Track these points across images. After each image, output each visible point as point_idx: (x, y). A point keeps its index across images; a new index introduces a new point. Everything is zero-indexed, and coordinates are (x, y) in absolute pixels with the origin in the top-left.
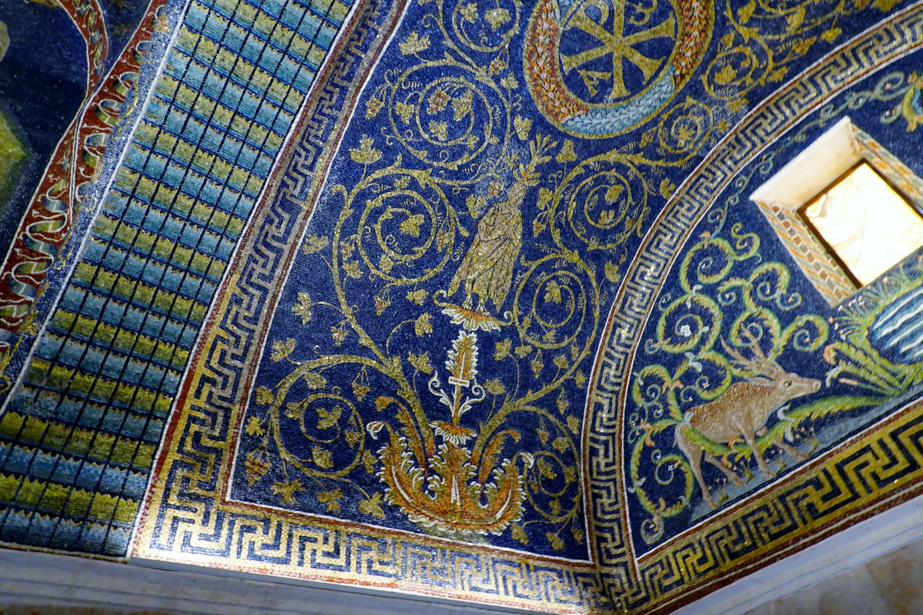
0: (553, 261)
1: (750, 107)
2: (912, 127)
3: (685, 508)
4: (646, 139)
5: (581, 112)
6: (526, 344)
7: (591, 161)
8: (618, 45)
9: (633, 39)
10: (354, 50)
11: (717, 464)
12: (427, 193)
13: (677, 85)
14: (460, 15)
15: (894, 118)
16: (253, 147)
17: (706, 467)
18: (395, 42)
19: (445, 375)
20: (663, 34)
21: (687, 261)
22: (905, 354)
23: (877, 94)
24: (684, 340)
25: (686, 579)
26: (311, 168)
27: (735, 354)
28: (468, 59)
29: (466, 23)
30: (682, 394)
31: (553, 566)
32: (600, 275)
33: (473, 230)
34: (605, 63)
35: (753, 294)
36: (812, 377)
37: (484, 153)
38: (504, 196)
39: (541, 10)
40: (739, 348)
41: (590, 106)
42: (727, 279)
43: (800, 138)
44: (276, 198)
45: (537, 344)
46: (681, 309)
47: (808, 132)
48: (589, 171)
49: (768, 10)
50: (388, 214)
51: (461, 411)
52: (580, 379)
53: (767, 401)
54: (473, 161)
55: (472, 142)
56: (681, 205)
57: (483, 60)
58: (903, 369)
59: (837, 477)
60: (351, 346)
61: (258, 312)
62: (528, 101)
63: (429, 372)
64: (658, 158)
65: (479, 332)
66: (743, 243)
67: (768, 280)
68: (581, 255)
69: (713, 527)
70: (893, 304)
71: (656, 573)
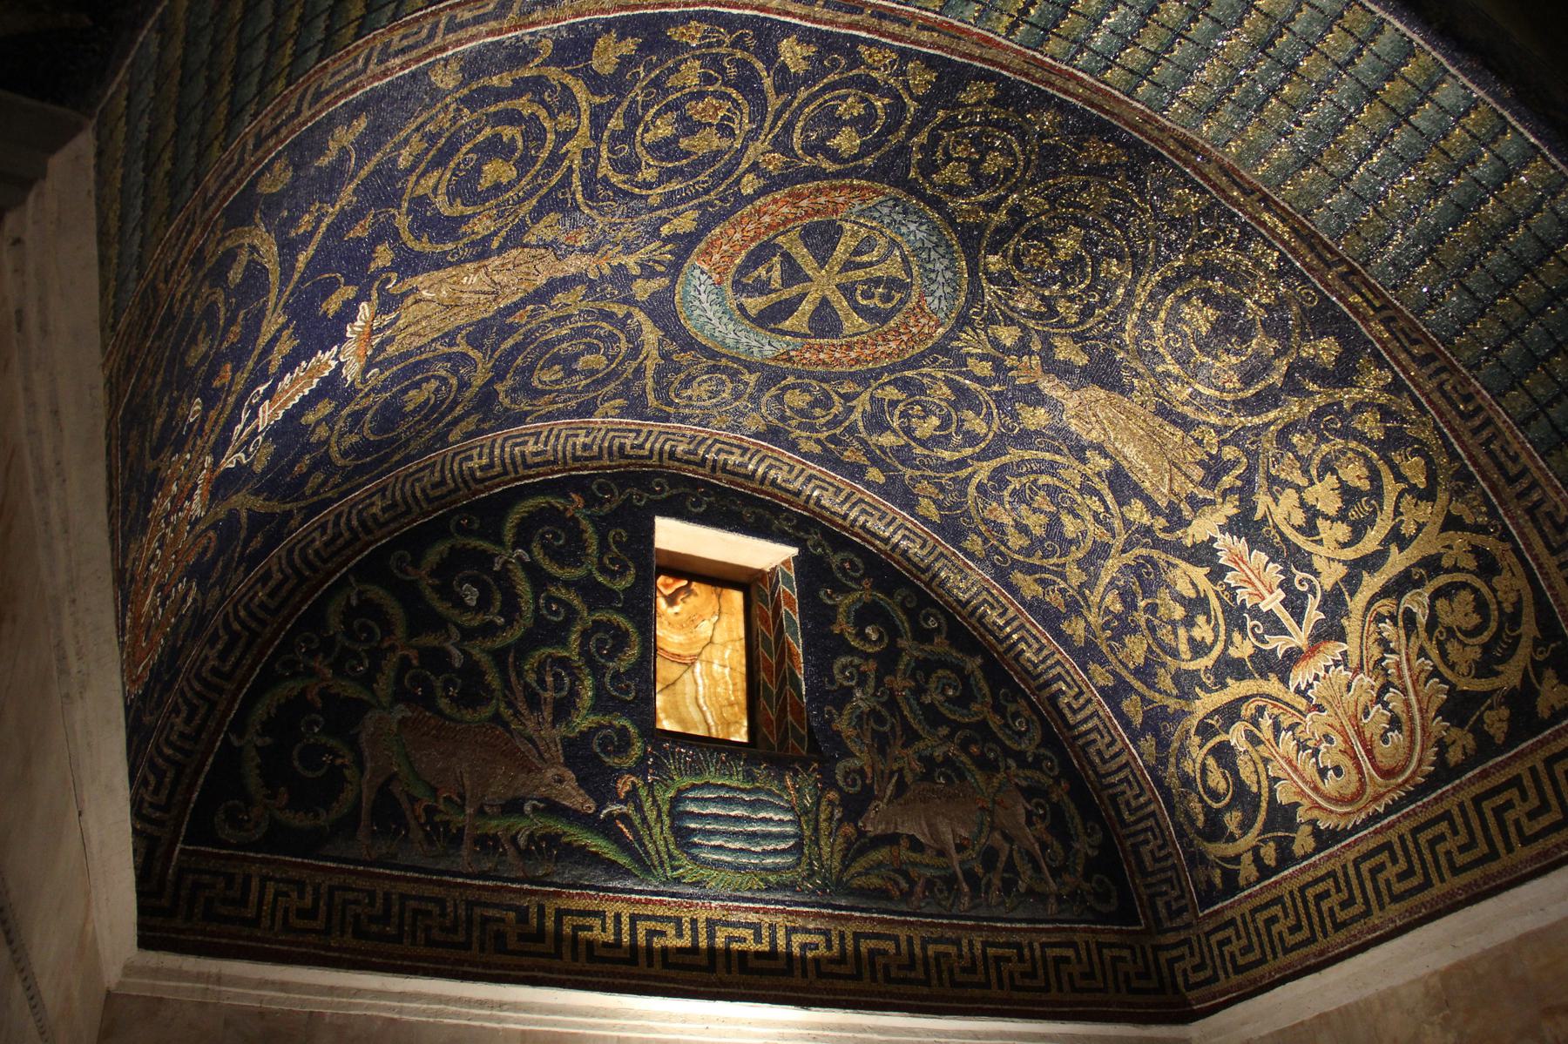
1: (757, 435)
5: (716, 277)
7: (640, 316)
8: (822, 283)
11: (405, 805)
12: (555, 160)
13: (775, 359)
14: (844, 98)
19: (269, 394)
20: (846, 324)
22: (696, 845)
23: (835, 560)
25: (266, 922)
28: (780, 124)
29: (835, 108)
30: (411, 672)
32: (456, 422)
33: (502, 249)
34: (793, 273)
35: (585, 635)
36: (590, 793)
37: (633, 196)
39: (861, 188)
40: (527, 686)
42: (567, 584)
43: (747, 513)
47: (759, 518)
48: (622, 324)
49: (897, 412)
50: (508, 132)
55: (648, 174)
57: (781, 144)
58: (684, 860)
59: (550, 924)
62: (724, 216)
65: (341, 365)
66: (612, 561)
67: (613, 637)
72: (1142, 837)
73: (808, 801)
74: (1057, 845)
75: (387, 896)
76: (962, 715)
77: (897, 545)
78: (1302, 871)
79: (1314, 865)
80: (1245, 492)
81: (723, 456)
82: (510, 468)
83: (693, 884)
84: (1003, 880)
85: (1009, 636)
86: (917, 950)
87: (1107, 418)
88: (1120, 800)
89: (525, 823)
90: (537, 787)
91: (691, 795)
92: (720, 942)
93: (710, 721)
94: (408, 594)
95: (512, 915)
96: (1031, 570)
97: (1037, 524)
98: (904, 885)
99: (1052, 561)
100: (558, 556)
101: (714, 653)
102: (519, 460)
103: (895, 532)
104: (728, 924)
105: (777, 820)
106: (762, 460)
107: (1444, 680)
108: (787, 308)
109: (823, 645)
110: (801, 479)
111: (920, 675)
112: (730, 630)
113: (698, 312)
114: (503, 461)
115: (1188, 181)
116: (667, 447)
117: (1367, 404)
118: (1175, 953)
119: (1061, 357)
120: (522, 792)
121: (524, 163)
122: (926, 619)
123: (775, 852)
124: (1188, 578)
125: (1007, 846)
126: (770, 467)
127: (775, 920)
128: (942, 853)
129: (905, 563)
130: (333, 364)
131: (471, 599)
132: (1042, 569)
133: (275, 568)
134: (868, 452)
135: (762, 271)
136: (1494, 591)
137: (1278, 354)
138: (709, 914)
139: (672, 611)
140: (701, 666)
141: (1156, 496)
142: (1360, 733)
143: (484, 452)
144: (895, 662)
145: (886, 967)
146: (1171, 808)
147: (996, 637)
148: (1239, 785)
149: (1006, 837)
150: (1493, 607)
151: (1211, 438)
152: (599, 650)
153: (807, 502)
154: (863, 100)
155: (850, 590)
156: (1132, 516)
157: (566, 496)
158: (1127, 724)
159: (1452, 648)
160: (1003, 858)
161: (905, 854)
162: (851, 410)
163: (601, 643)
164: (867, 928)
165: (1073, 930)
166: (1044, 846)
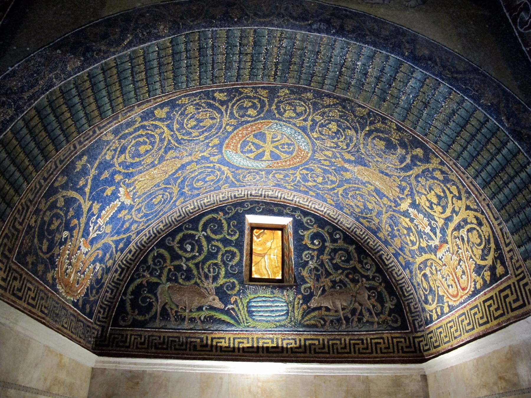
0: (169, 188)
1: (273, 186)
2: (304, 243)
3: (146, 320)
4: (240, 171)
7: (217, 165)
14: (244, 102)
15: (302, 234)
17: (164, 309)
20: (281, 156)
22: (254, 315)
23: (305, 220)
24: (186, 251)
25: (132, 347)
27: (202, 274)
28: (228, 113)
30: (171, 273)
31: (84, 320)
32: (175, 201)
34: (258, 147)
35: (223, 255)
36: (223, 302)
39: (264, 122)
40: (205, 273)
41: (239, 152)
42: (217, 240)
43: (276, 209)
45: (134, 217)
46: (193, 236)
50: (141, 140)
51: (93, 236)
52: (133, 237)
56: (222, 194)
58: (250, 320)
59: (209, 342)
60: (81, 191)
61: (66, 158)
64: (235, 178)
65: (123, 203)
66: (232, 231)
68: (179, 191)
69: (155, 334)
70: (261, 297)
71: (118, 338)
72: (410, 301)
74: (379, 306)
75: (164, 337)
76: (347, 265)
77: (326, 212)
78: (446, 318)
79: (449, 317)
80: (412, 194)
81: (267, 193)
82: (201, 207)
83: (253, 327)
84: (358, 318)
85: (364, 238)
86: (326, 343)
88: (404, 288)
89: (203, 313)
90: (207, 302)
91: (253, 300)
92: (260, 345)
93: (270, 273)
94: (170, 249)
95: (199, 340)
96: (364, 218)
98: (322, 322)
99: (369, 215)
100: (215, 232)
101: (272, 252)
102: (203, 205)
103: (324, 208)
104: (263, 339)
105: (281, 306)
106: (279, 192)
107: (473, 260)
108: (262, 155)
109: (300, 248)
110: (292, 196)
111: (332, 254)
112: (277, 244)
113: (235, 161)
114: (198, 206)
116: (249, 193)
117: (436, 169)
118: (420, 339)
120: (203, 304)
121: (152, 144)
122: (336, 235)
123: (279, 316)
124: (405, 221)
125: (360, 307)
126: (282, 194)
127: (278, 336)
128: (336, 311)
129: (329, 218)
130: (120, 203)
131: (189, 249)
132: (367, 218)
133: (132, 249)
134: (307, 187)
136: (482, 231)
137: (407, 153)
139: (258, 240)
140: (267, 257)
141: (389, 197)
142: (456, 274)
143: (191, 206)
144: (324, 251)
145: (315, 349)
146: (416, 292)
147: (360, 238)
149: (361, 305)
150: (483, 237)
152: (227, 259)
153: (295, 202)
154: (251, 101)
156: (385, 202)
157: (218, 213)
158: (401, 265)
159: (474, 249)
160: (359, 311)
161: (324, 312)
162: (296, 177)
163: (228, 257)
164: (309, 337)
165: (383, 333)
166: (374, 306)
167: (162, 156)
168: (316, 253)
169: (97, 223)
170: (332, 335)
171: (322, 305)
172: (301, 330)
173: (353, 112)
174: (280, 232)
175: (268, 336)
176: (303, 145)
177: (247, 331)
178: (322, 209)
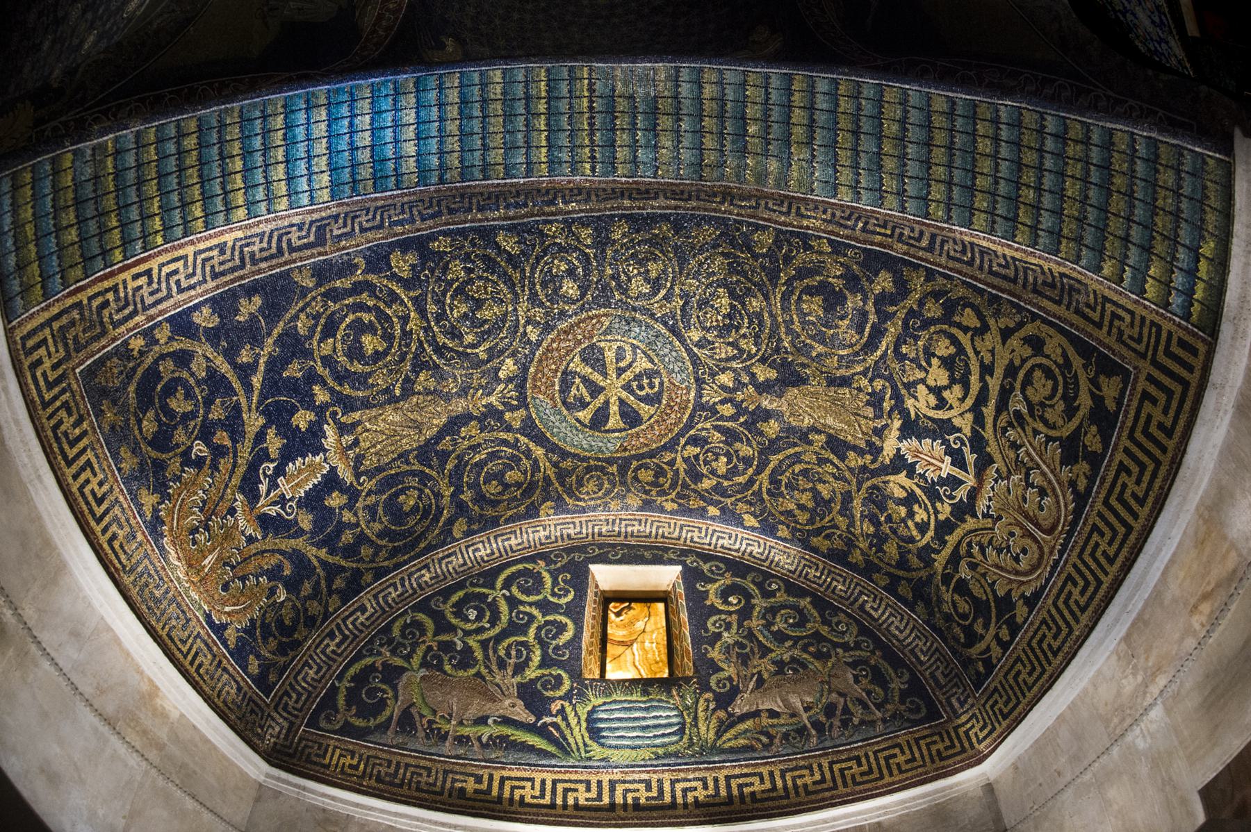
0: (430, 478)
1: (641, 509)
2: (708, 603)
6: (356, 514)
8: (614, 389)
9: (624, 394)
10: (474, 201)
12: (406, 334)
16: (353, 175)
18: (502, 228)
19: (280, 471)
21: (514, 569)
22: (604, 737)
23: (706, 567)
24: (467, 620)
26: (363, 230)
29: (550, 271)
32: (450, 522)
34: (595, 390)
35: (539, 629)
36: (533, 712)
38: (448, 398)
40: (499, 657)
42: (530, 604)
44: (323, 219)
48: (515, 445)
50: (366, 317)
53: (490, 705)
54: (456, 352)
55: (469, 338)
56: (545, 529)
58: (595, 746)
59: (496, 784)
60: (245, 372)
63: (272, 456)
65: (333, 470)
68: (452, 495)
69: (379, 754)
70: (620, 702)
73: (689, 702)
81: (629, 529)
87: (807, 406)
94: (438, 617)
97: (805, 498)
98: (765, 740)
99: (827, 519)
100: (527, 592)
101: (647, 637)
104: (624, 782)
105: (667, 715)
106: (652, 525)
112: (656, 623)
115: (758, 228)
119: (761, 379)
122: (770, 585)
123: (663, 735)
124: (898, 484)
126: (658, 527)
127: (661, 776)
132: (824, 528)
134: (703, 498)
135: (574, 391)
138: (612, 777)
140: (638, 648)
141: (858, 442)
148: (976, 601)
151: (864, 382)
155: (716, 581)
156: (852, 464)
164: (737, 771)
165: (897, 737)
167: (407, 380)
168: (735, 617)
169: (278, 486)
170: (790, 760)
171: (761, 707)
172: (716, 759)
173: (749, 249)
174: (660, 606)
175: (636, 777)
176: (677, 369)
177: (585, 767)
178: (737, 546)
